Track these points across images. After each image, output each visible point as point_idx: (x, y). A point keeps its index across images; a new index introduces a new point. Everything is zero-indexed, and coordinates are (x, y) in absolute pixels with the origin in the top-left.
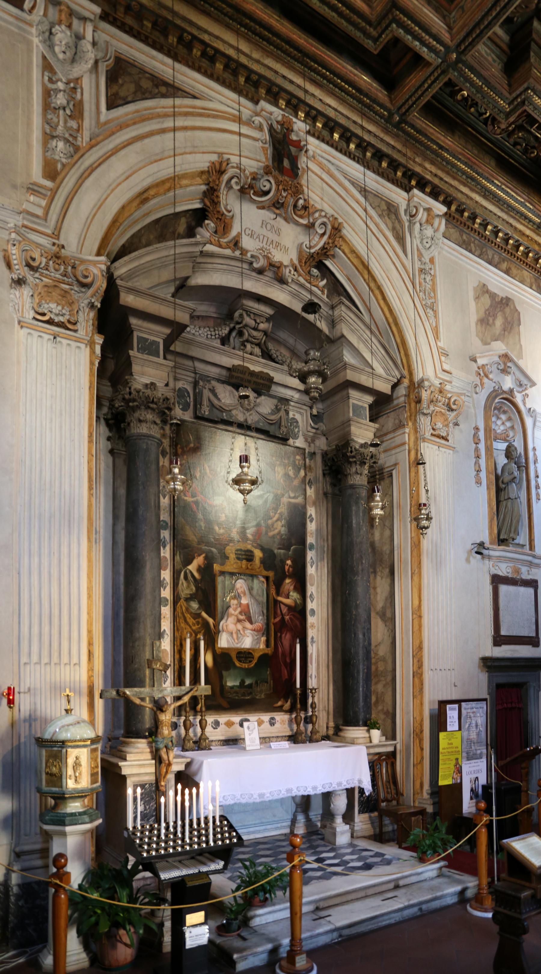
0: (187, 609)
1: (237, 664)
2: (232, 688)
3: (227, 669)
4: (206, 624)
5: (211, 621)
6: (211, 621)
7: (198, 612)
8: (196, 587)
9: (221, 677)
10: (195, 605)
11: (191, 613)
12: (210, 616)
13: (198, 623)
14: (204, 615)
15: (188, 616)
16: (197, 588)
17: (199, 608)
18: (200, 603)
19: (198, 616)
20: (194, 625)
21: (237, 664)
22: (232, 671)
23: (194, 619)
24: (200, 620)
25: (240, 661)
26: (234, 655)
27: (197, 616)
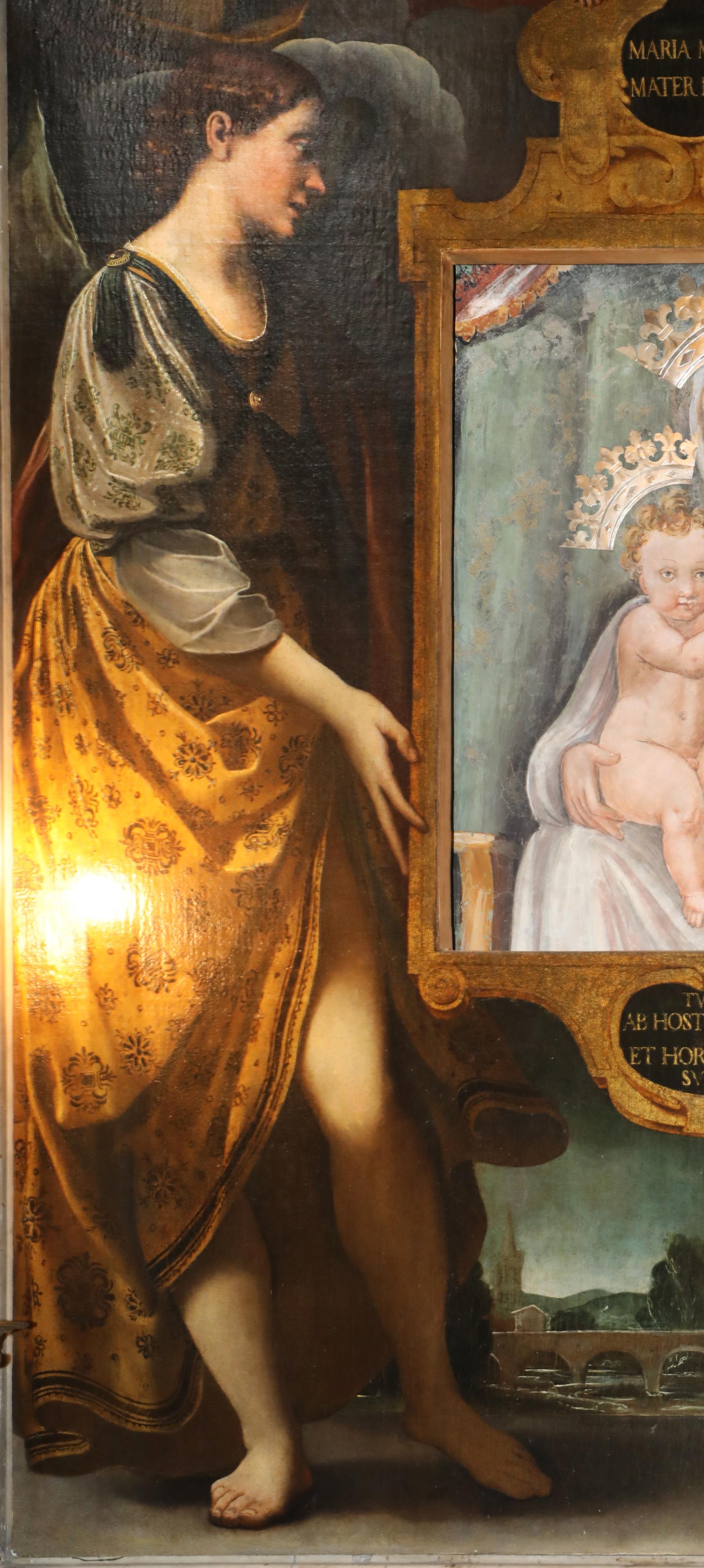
0: (128, 624)
1: (635, 1098)
2: (572, 1316)
3: (531, 1142)
4: (320, 748)
5: (365, 719)
6: (365, 719)
7: (240, 642)
8: (209, 417)
9: (463, 1222)
10: (202, 586)
11: (164, 661)
12: (354, 678)
13: (235, 743)
14: (297, 666)
15: (137, 685)
16: (227, 423)
17: (245, 611)
18: (251, 556)
19: (244, 675)
20: (195, 757)
21: (635, 1098)
22: (573, 1163)
23: (200, 706)
24: (255, 716)
25: (669, 1077)
26: (596, 1025)
27: (221, 681)
